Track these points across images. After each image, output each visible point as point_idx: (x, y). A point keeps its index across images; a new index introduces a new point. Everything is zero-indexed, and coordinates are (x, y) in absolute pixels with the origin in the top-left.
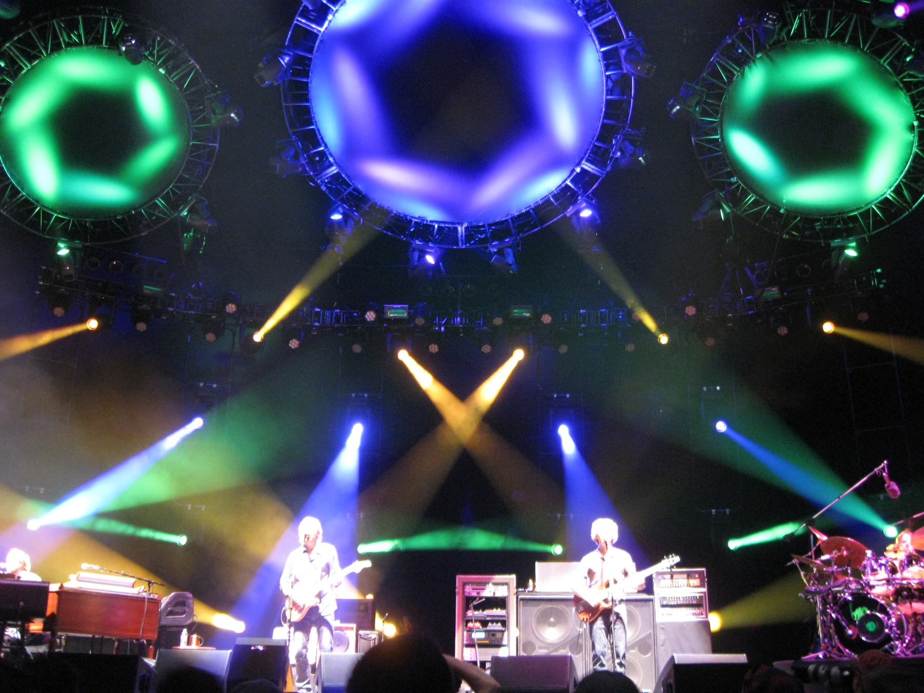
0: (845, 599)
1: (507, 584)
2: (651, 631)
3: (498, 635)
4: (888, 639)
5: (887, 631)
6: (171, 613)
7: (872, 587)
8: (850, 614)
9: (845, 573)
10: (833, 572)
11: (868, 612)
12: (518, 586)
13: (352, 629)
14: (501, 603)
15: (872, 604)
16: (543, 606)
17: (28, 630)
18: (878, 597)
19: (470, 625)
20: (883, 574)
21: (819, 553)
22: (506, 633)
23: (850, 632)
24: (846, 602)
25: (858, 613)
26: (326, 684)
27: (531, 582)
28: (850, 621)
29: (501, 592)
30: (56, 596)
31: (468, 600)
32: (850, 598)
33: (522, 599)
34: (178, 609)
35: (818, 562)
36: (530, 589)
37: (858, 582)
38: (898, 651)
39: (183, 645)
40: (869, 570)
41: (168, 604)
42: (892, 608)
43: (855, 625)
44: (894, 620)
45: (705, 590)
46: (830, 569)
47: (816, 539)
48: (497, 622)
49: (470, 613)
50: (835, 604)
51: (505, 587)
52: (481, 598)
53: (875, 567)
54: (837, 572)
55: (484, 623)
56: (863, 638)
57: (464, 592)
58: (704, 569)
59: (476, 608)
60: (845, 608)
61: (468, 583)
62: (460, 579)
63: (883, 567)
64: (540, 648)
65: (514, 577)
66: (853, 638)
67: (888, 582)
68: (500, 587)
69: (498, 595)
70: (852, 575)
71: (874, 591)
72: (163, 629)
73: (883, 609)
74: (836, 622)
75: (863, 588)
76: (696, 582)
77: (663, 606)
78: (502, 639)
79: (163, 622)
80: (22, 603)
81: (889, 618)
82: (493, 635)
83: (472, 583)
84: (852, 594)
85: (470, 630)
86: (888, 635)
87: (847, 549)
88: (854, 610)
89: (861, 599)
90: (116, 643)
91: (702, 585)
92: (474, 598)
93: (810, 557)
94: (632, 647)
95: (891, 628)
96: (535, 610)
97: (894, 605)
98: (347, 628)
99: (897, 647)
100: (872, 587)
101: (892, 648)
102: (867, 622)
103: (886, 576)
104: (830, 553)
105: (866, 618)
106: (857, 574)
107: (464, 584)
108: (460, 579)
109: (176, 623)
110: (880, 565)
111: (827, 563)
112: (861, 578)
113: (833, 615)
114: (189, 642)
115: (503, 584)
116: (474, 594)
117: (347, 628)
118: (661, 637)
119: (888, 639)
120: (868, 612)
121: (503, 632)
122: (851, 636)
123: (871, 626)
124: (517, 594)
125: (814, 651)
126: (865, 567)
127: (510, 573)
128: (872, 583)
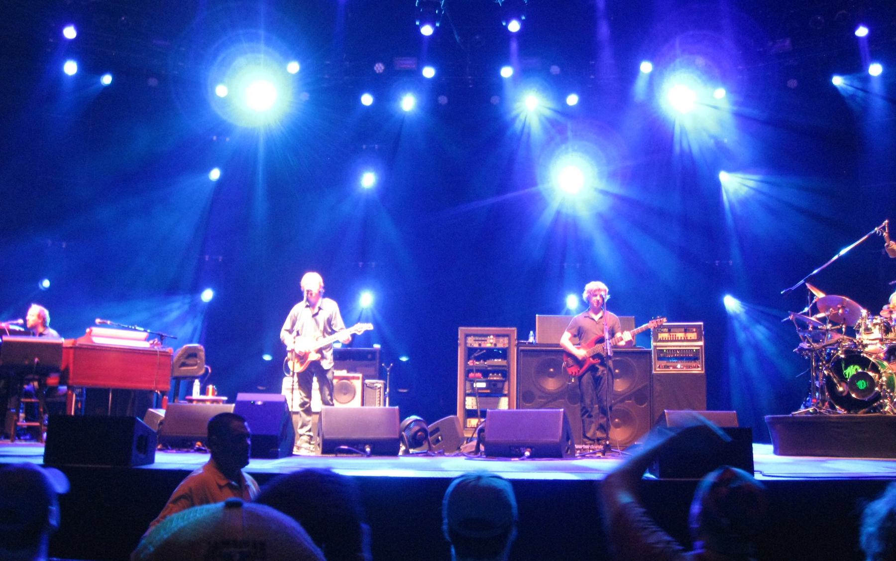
0: (838, 356)
1: (507, 336)
2: (648, 383)
3: (499, 385)
4: (878, 397)
5: (877, 389)
6: (184, 365)
7: (866, 345)
8: (842, 371)
9: (839, 331)
10: (827, 330)
11: (860, 370)
12: (519, 338)
13: (358, 378)
14: (503, 354)
15: (864, 362)
16: (544, 357)
17: (45, 385)
18: (871, 354)
19: (471, 375)
20: (877, 333)
21: (815, 310)
22: (506, 384)
23: (841, 389)
24: (839, 360)
25: (851, 371)
26: (326, 437)
27: (531, 332)
28: (842, 378)
29: (502, 343)
30: (72, 351)
31: (470, 352)
32: (843, 356)
33: (522, 351)
34: (191, 361)
35: (813, 319)
36: (531, 340)
37: (852, 341)
38: (887, 409)
39: (196, 393)
40: (862, 330)
41: (182, 355)
42: (883, 366)
43: (846, 383)
44: (884, 379)
45: (701, 343)
46: (824, 327)
47: (813, 295)
48: (497, 372)
49: (470, 363)
50: (828, 362)
51: (506, 340)
52: (482, 349)
53: (869, 326)
54: (832, 330)
55: (485, 373)
56: (854, 395)
57: (466, 343)
58: (701, 323)
59: (478, 359)
60: (838, 367)
61: (470, 335)
62: (462, 331)
63: (877, 327)
64: (540, 397)
65: (515, 329)
66: (844, 394)
67: (881, 340)
68: (501, 340)
69: (500, 345)
70: (847, 333)
71: (867, 349)
72: (178, 379)
73: (875, 368)
74: (828, 378)
75: (856, 347)
76: (693, 336)
77: (660, 359)
78: (502, 388)
79: (176, 374)
80: (36, 360)
81: (880, 377)
82: (495, 385)
83: (475, 335)
84: (846, 352)
85: (472, 381)
86: (878, 394)
87: (843, 307)
88: (846, 368)
89: (855, 356)
90: (133, 394)
91: (698, 340)
92: (475, 350)
93: (807, 314)
94: (629, 398)
95: (882, 385)
96: (535, 361)
97: (885, 363)
98: (353, 378)
99: (886, 405)
100: (866, 345)
101: (882, 406)
102: (858, 380)
103: (880, 336)
104: (827, 310)
105: (858, 377)
106: (852, 332)
107: (467, 336)
108: (462, 331)
109: (189, 374)
110: (875, 325)
111: (823, 320)
112: (855, 337)
113: (826, 372)
114: (203, 391)
115: (504, 336)
116: (476, 345)
117: (353, 378)
118: (658, 387)
119: (878, 397)
120: (860, 370)
121: (503, 382)
122: (842, 392)
123: (862, 384)
124: (518, 345)
125: (806, 407)
126: (859, 326)
127: (511, 326)
128: (865, 342)
